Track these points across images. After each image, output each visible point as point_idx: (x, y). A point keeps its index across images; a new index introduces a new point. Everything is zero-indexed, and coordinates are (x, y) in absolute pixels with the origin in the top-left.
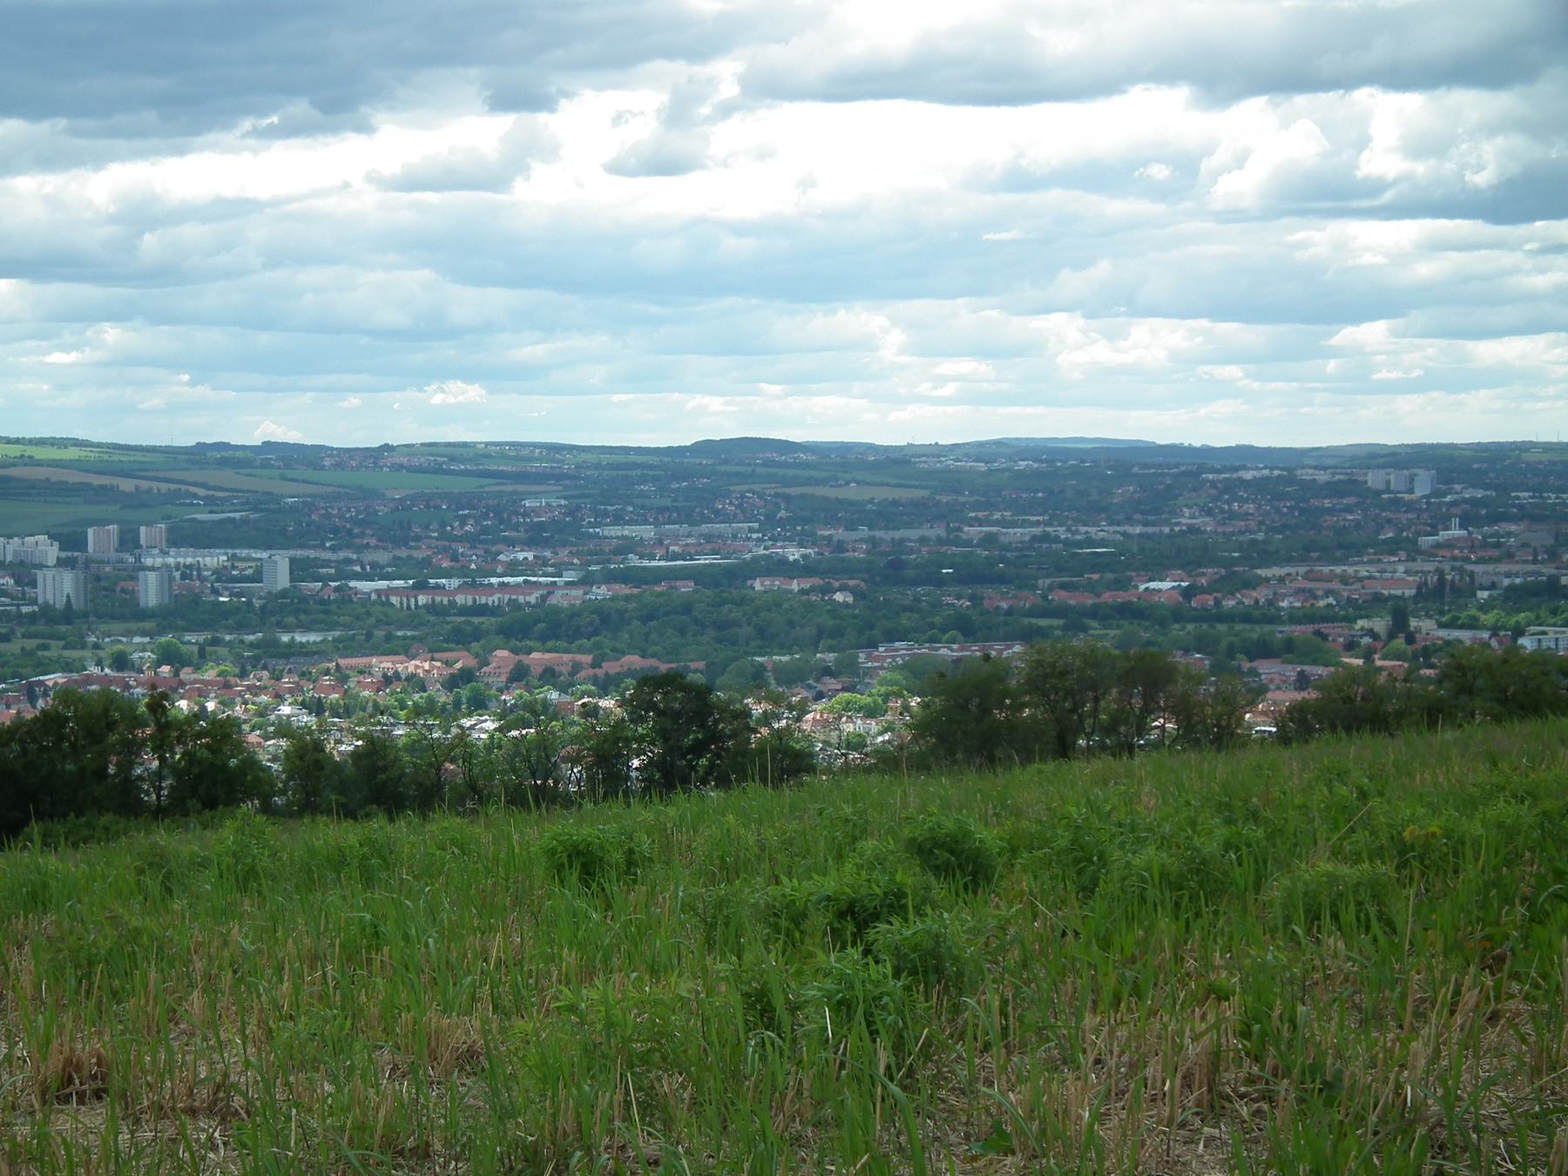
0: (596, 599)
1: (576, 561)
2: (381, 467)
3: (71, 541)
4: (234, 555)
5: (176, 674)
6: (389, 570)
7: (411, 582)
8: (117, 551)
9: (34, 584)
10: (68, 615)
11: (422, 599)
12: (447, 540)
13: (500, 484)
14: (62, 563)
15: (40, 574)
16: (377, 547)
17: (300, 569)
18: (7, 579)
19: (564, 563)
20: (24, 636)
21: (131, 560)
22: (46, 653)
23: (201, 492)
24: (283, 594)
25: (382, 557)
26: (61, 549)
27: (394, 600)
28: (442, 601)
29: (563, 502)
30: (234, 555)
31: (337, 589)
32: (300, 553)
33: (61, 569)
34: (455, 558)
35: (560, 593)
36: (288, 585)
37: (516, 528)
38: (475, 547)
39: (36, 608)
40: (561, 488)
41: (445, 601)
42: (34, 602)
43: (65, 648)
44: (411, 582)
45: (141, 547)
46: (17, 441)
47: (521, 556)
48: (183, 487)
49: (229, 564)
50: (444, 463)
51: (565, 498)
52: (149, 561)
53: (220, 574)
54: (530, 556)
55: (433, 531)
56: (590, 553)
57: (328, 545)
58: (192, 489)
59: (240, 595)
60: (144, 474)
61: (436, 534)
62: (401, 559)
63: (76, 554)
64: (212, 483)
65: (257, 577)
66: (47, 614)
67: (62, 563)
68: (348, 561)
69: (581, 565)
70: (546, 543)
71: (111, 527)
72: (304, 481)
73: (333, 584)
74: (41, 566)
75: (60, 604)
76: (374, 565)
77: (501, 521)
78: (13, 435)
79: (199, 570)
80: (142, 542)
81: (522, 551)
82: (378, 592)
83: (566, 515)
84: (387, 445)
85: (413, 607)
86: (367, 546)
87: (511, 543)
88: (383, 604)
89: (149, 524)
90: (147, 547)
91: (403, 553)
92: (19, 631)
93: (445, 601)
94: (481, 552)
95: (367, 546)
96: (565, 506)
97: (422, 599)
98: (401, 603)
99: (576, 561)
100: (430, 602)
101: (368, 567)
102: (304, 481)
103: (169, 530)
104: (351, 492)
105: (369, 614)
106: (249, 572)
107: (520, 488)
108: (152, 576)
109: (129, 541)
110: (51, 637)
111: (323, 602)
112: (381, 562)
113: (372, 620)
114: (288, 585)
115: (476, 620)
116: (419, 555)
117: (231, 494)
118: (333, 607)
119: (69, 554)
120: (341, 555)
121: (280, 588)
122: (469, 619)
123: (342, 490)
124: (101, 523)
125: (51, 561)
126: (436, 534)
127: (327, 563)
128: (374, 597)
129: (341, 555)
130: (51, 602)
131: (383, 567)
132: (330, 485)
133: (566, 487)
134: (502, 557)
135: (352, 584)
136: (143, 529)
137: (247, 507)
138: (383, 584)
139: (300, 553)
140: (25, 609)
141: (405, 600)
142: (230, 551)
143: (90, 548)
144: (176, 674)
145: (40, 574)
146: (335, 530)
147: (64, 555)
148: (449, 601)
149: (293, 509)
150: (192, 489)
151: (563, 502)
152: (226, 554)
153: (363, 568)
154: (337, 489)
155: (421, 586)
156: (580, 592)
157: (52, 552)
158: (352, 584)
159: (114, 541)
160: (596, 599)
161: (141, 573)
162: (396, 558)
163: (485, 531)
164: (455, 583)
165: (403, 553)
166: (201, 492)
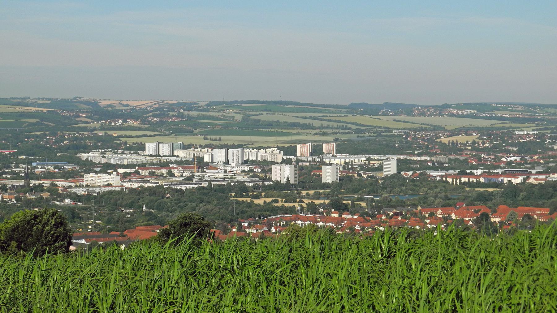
0: (552, 180)
1: (542, 161)
2: (443, 116)
3: (290, 151)
4: (369, 157)
5: (340, 216)
6: (447, 165)
7: (458, 171)
8: (311, 155)
9: (271, 171)
10: (287, 186)
11: (464, 179)
12: (476, 151)
13: (503, 123)
14: (283, 161)
15: (273, 167)
16: (440, 154)
17: (402, 165)
18: (258, 169)
19: (536, 163)
20: (265, 196)
21: (318, 159)
22: (276, 204)
23: (354, 127)
24: (393, 176)
25: (443, 158)
26: (284, 155)
27: (450, 180)
28: (473, 180)
29: (536, 132)
30: (369, 157)
31: (420, 174)
32: (402, 157)
33: (284, 165)
34: (480, 159)
35: (533, 177)
36: (396, 172)
37: (512, 145)
38: (490, 155)
39: (271, 183)
40: (534, 125)
41: (475, 181)
42: (270, 179)
43: (285, 202)
44: (458, 171)
45: (323, 153)
46: (263, 102)
47: (513, 159)
48: (345, 125)
49: (367, 162)
50: (475, 113)
51: (537, 130)
52: (327, 161)
53: (362, 167)
54: (518, 159)
55: (469, 146)
56: (549, 157)
57: (416, 152)
58: (349, 126)
59: (372, 177)
60: (325, 118)
61: (470, 148)
62: (452, 159)
63: (291, 157)
64: (359, 123)
65: (380, 169)
66: (277, 185)
67: (283, 161)
68: (426, 161)
69: (544, 163)
70: (526, 152)
71: (308, 144)
72: (404, 122)
73: (418, 172)
74: (274, 163)
75: (283, 181)
76: (439, 162)
77: (504, 141)
78: (261, 100)
79: (352, 165)
80: (324, 150)
81: (514, 156)
82: (441, 176)
83: (537, 138)
84: (446, 104)
85: (458, 183)
86: (436, 154)
87: (509, 152)
88: (444, 182)
89: (327, 142)
90: (326, 153)
91: (453, 157)
92: (263, 194)
93: (475, 181)
94: (493, 157)
95: (436, 154)
96: (537, 134)
97: (464, 179)
98: (453, 181)
99: (542, 161)
100: (467, 181)
101: (436, 164)
102: (404, 122)
103: (337, 146)
104: (428, 127)
105: (436, 187)
106: (376, 166)
107: (513, 125)
108: (329, 167)
109: (317, 151)
110: (279, 197)
111: (413, 180)
112: (444, 161)
113: (438, 190)
114: (396, 172)
115: (490, 190)
116: (461, 158)
117: (368, 128)
118: (418, 183)
119: (288, 157)
120: (422, 158)
121: (392, 173)
122: (487, 189)
123: (424, 126)
124: (304, 142)
125: (279, 160)
126: (470, 148)
127: (415, 162)
128: (438, 178)
129: (422, 158)
130: (279, 180)
131: (443, 164)
132: (419, 124)
133: (537, 125)
134: (503, 159)
135: (428, 172)
136: (324, 145)
137: (375, 135)
138: (443, 173)
139: (402, 157)
140: (267, 183)
141: (454, 180)
142: (367, 156)
143: (298, 154)
144: (340, 216)
145: (273, 167)
146: (420, 146)
147: (285, 157)
148: (476, 180)
149: (399, 136)
150: (349, 126)
151: (536, 132)
152: (365, 157)
153: (434, 164)
154: (420, 126)
155: (463, 173)
156: (543, 177)
157: (278, 156)
158: (428, 172)
159: (310, 150)
160: (552, 180)
161: (323, 166)
162: (450, 159)
163: (495, 146)
164: (480, 172)
165: (453, 157)
166: (354, 127)
